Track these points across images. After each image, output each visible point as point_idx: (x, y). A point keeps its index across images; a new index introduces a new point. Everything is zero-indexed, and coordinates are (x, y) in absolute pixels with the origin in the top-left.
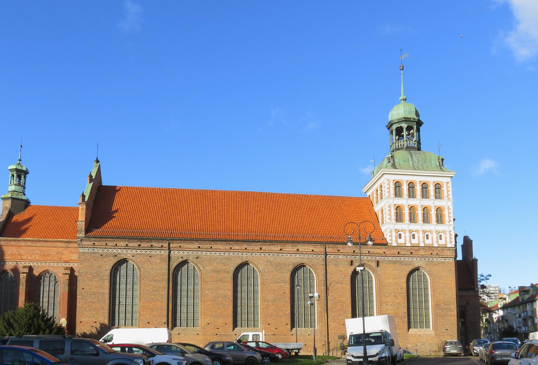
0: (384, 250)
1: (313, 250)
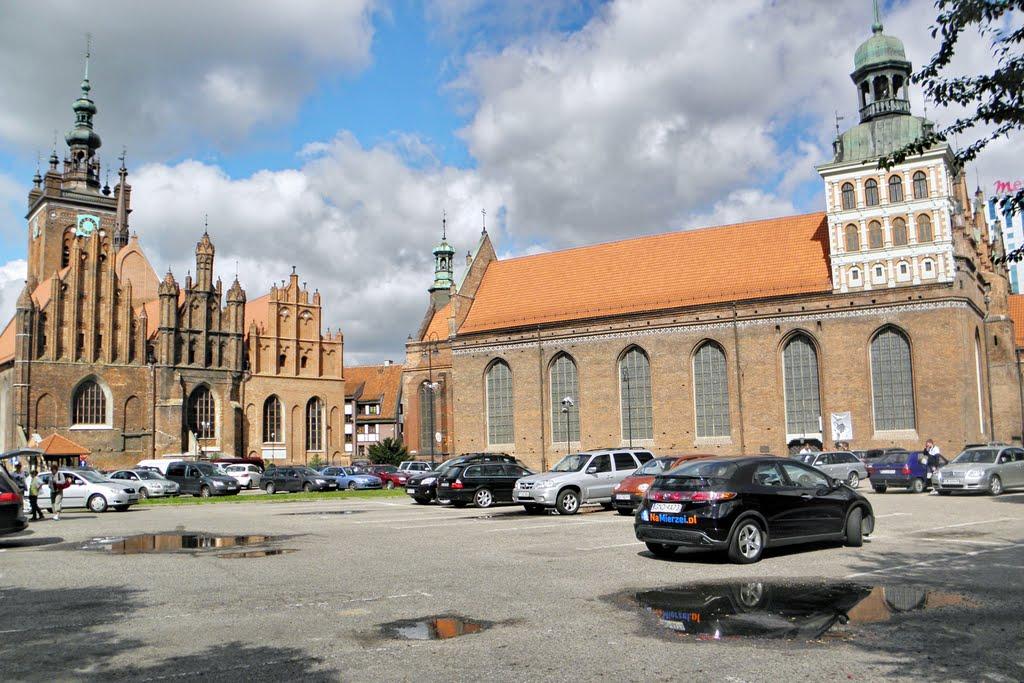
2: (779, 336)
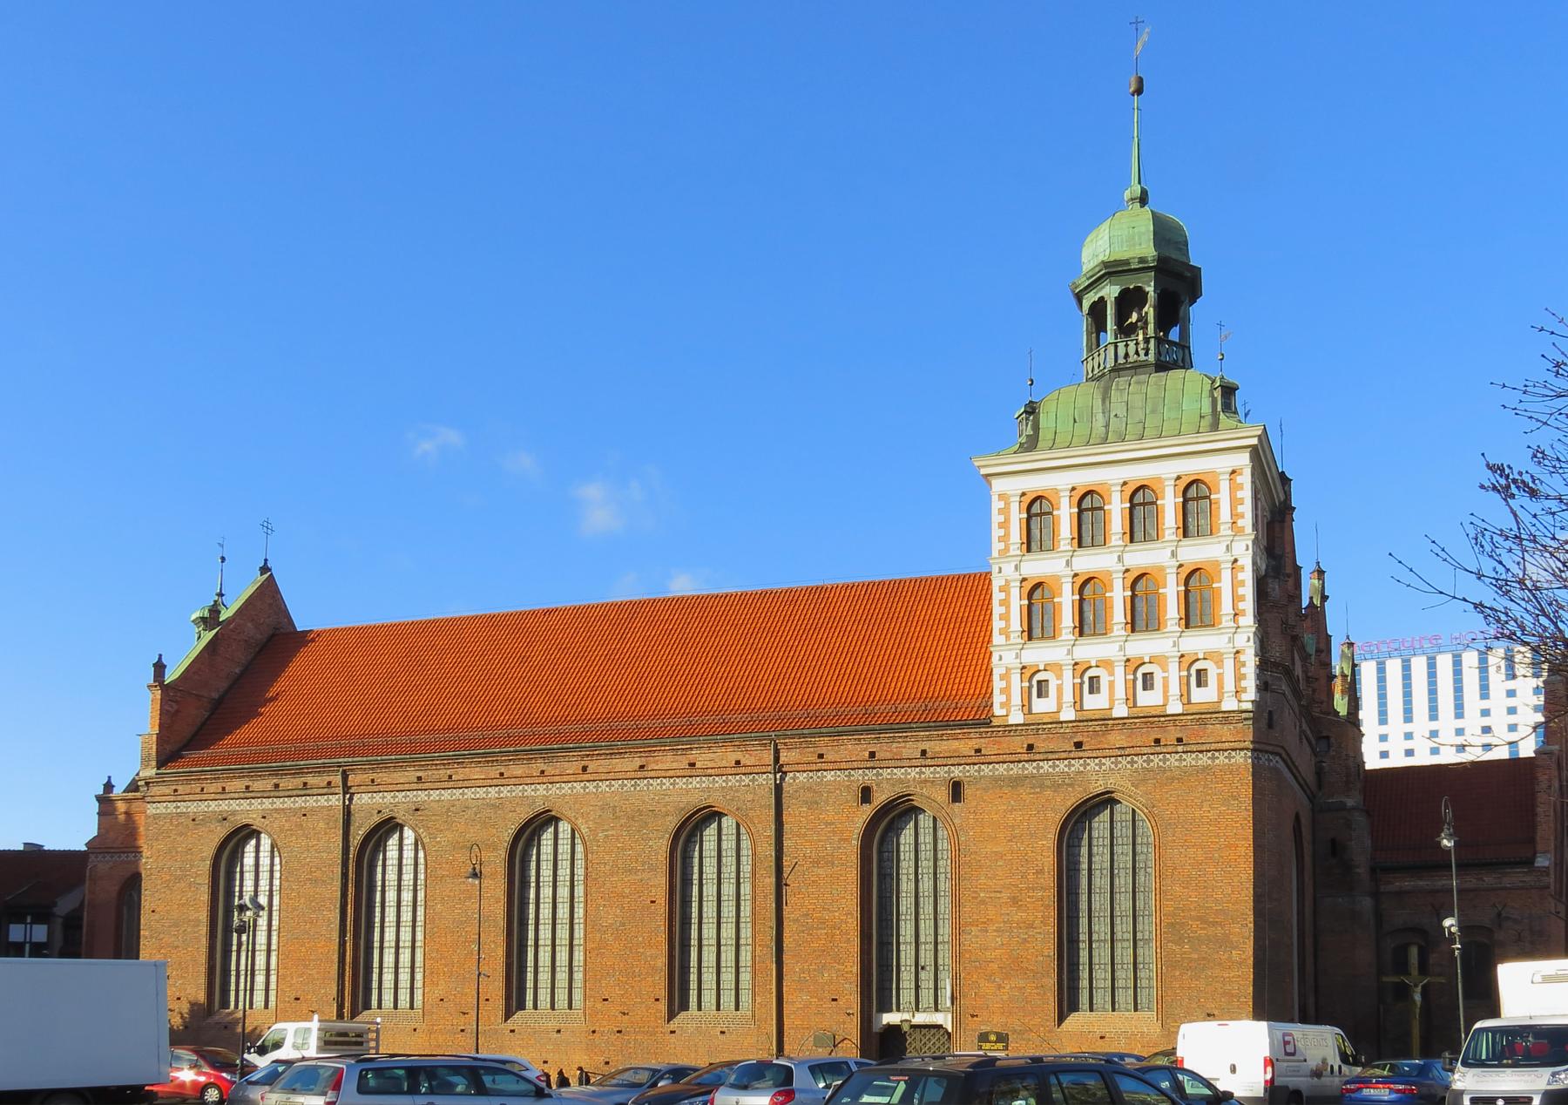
0: (975, 743)
1: (738, 762)
2: (867, 811)
